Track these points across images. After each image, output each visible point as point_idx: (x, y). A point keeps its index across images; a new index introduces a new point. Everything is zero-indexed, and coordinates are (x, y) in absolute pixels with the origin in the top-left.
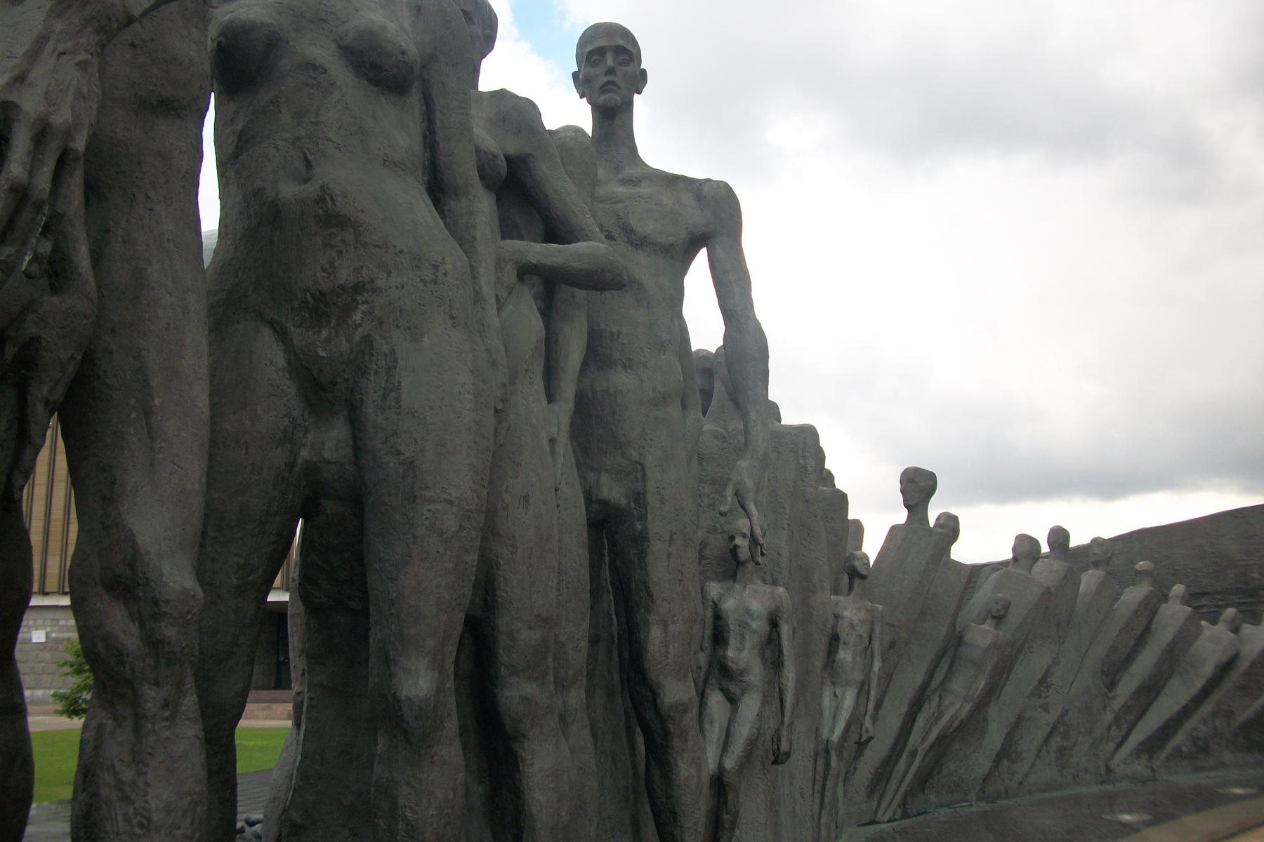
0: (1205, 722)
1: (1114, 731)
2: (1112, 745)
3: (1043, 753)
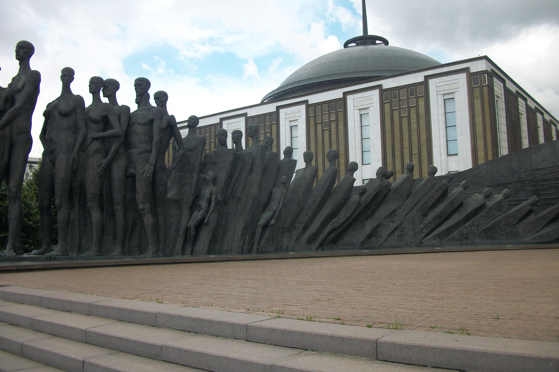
0: (467, 228)
1: (424, 230)
2: (423, 235)
3: (392, 236)
